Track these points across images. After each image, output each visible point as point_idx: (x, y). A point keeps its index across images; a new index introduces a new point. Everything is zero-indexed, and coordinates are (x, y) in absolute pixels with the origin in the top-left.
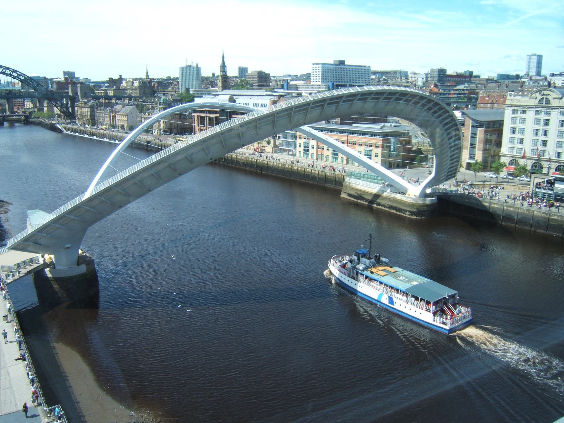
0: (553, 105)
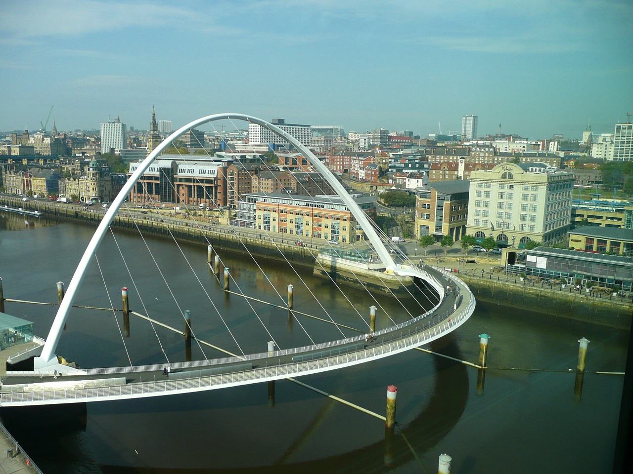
0: (515, 179)
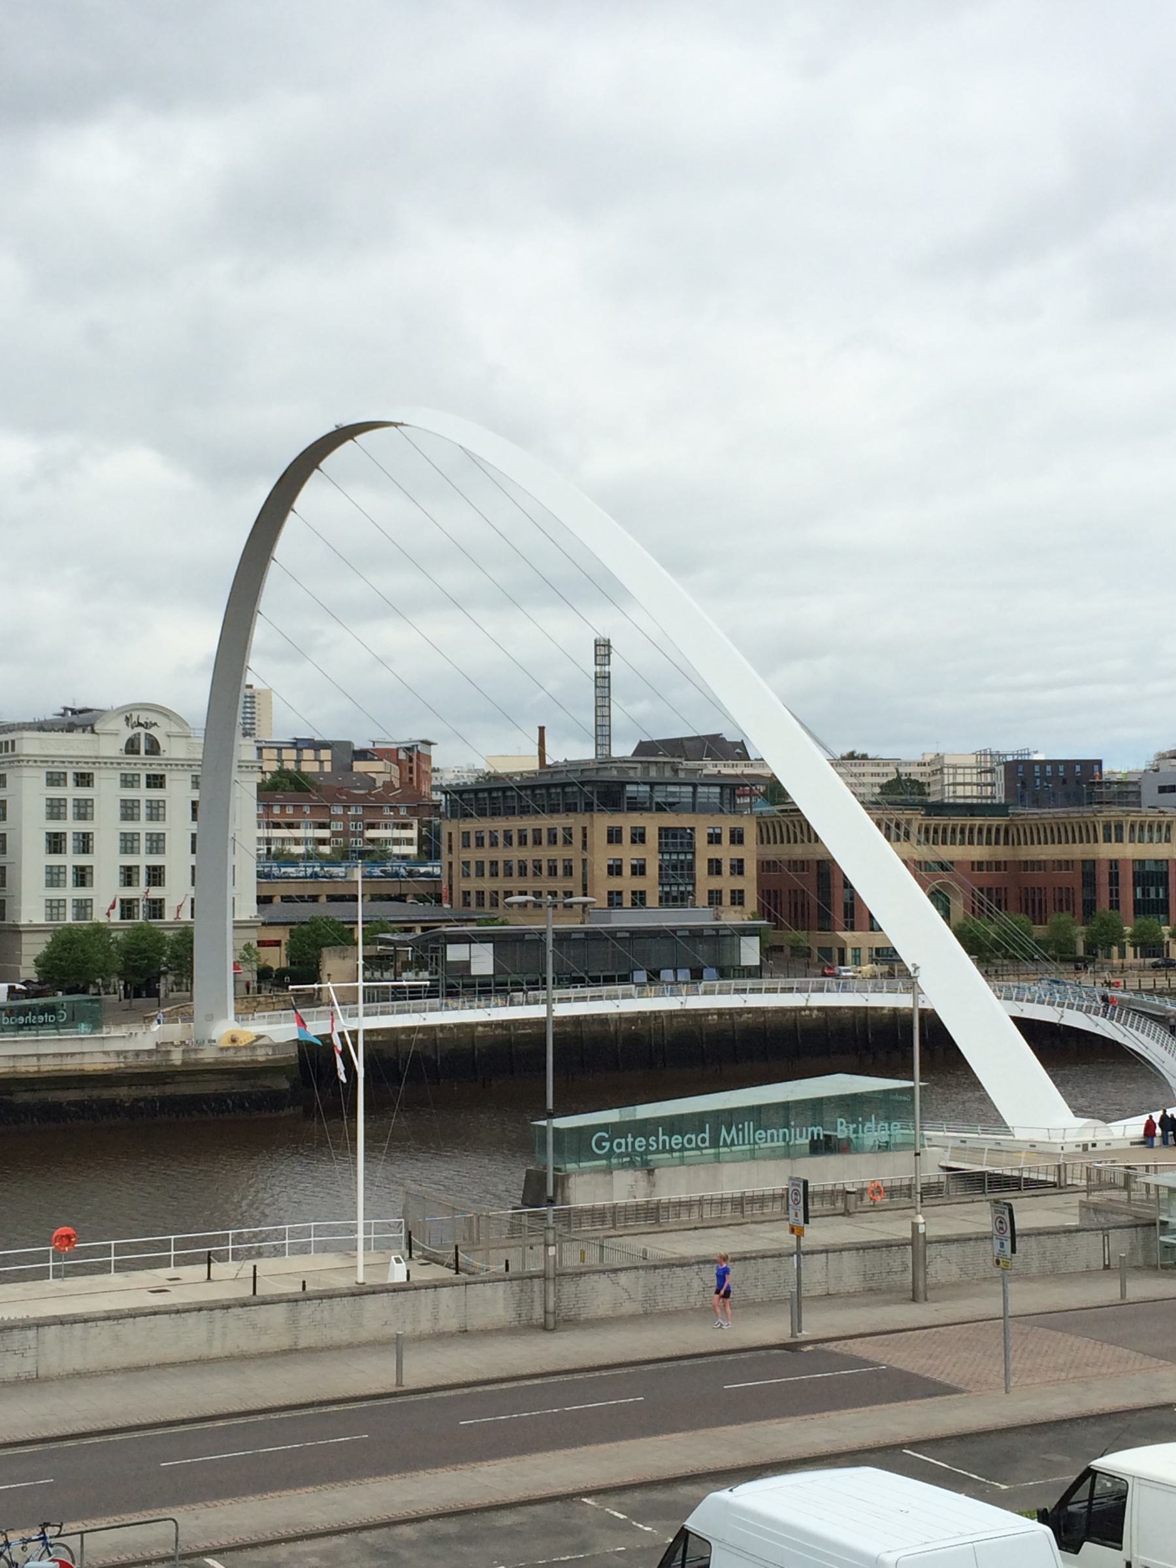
0: (166, 755)
